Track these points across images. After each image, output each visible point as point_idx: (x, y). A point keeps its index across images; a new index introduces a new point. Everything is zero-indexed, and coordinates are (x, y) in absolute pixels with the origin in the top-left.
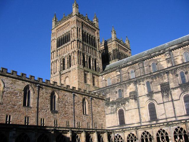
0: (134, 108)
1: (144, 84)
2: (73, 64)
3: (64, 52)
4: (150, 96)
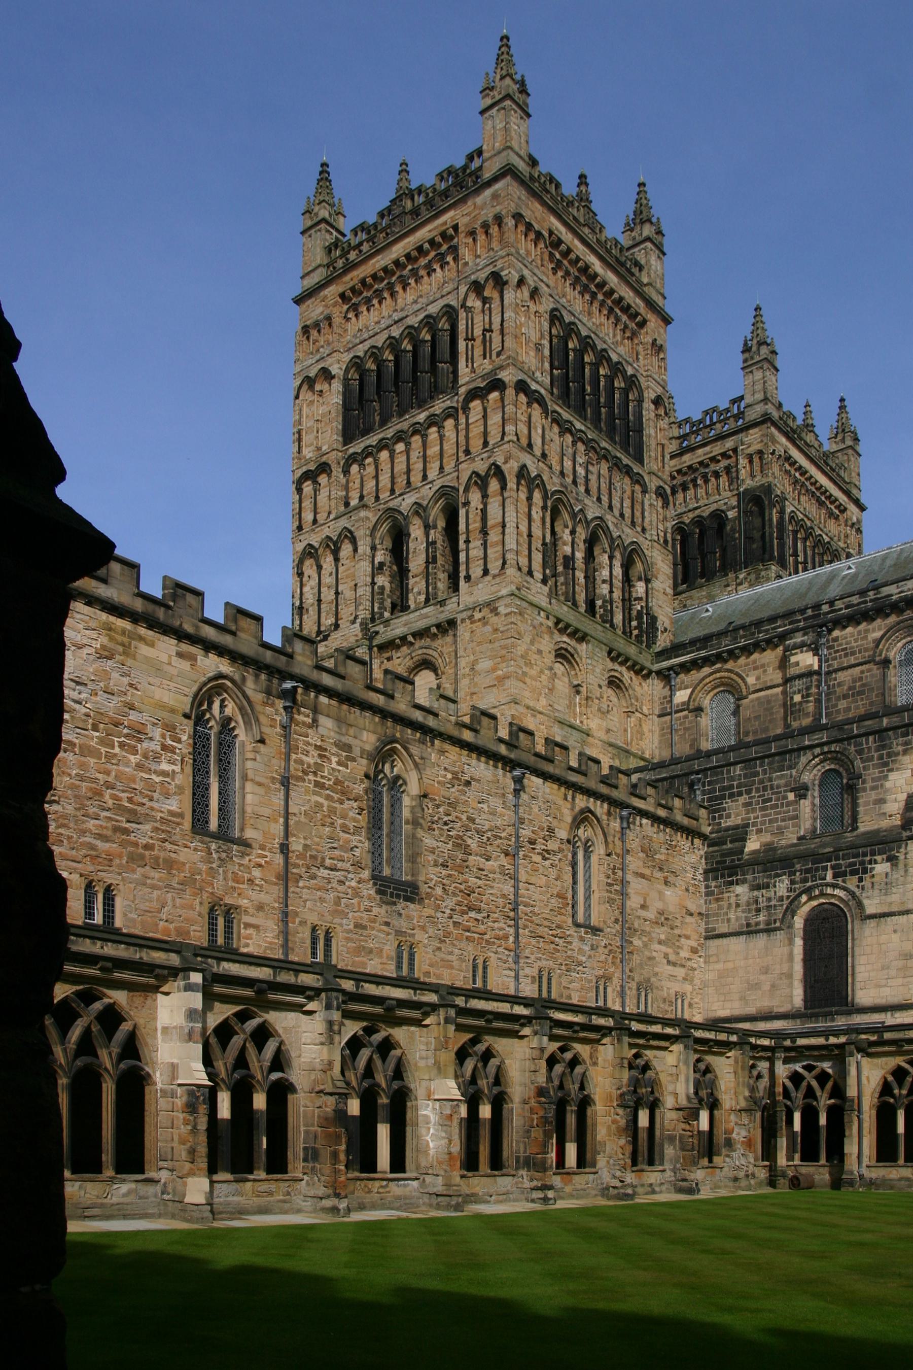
2: (476, 571)
3: (401, 481)
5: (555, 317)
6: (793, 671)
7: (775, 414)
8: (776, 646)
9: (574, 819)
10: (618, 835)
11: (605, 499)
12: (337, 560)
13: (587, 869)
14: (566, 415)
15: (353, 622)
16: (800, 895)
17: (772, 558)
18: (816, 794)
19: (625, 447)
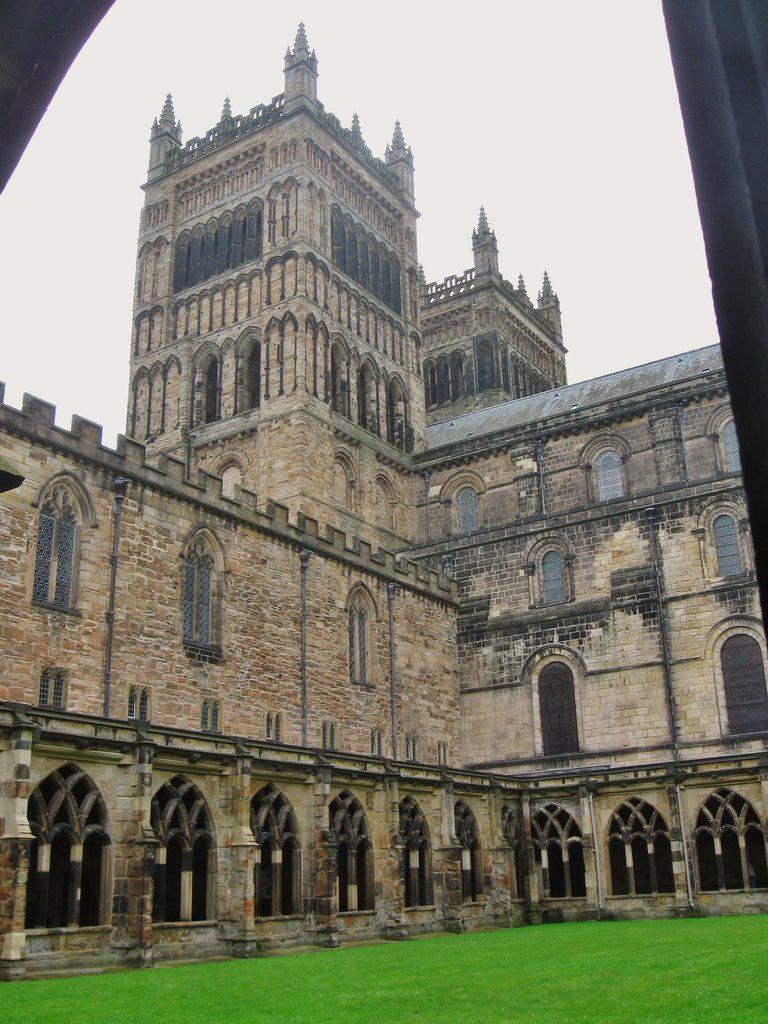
0: (634, 662)
1: (703, 531)
2: (274, 391)
3: (217, 321)
4: (734, 596)
5: (336, 210)
6: (520, 473)
7: (498, 283)
8: (505, 453)
9: (351, 591)
10: (386, 605)
11: (372, 340)
12: (165, 379)
13: (362, 633)
14: (343, 278)
15: (176, 428)
17: (499, 387)
18: (541, 571)
19: (387, 300)
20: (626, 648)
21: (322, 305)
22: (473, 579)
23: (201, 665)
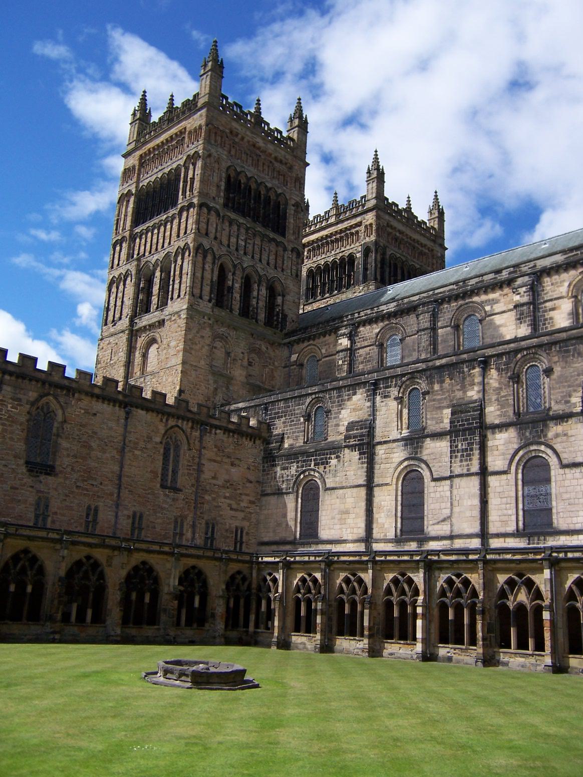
16: (300, 475)
20: (348, 473)
21: (212, 236)
22: (277, 422)
23: (38, 476)
